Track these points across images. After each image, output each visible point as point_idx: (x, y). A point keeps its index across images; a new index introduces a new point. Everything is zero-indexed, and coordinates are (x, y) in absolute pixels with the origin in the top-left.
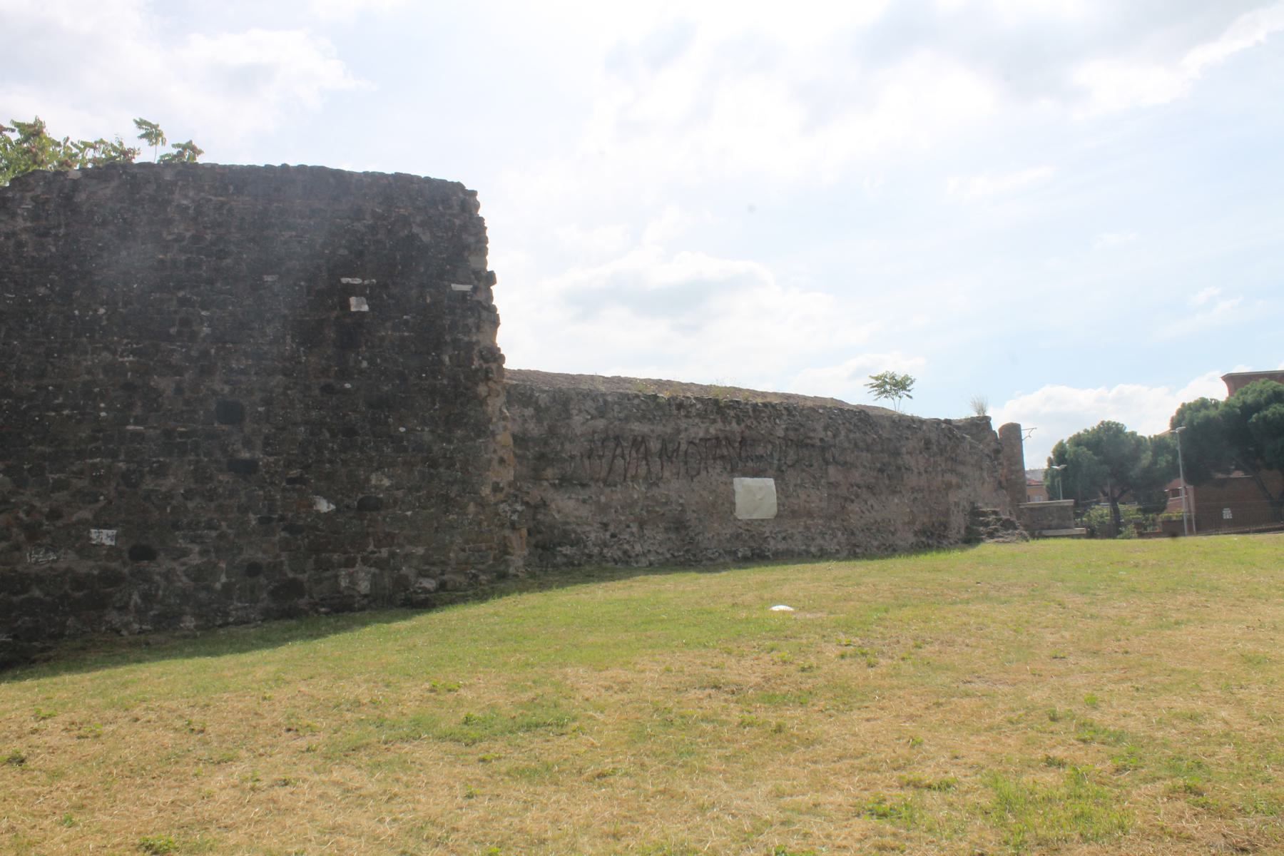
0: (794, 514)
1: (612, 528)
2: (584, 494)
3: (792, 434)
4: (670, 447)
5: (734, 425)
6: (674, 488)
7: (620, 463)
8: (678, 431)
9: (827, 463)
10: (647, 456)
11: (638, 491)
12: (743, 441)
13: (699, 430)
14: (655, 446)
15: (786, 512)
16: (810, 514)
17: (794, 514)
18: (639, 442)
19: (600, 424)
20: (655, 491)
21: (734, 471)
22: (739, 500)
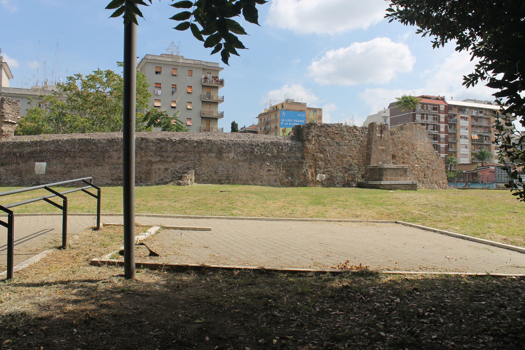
0: (50, 173)
1: (8, 176)
2: (5, 167)
3: (55, 149)
4: (22, 155)
5: (39, 148)
6: (23, 166)
7: (10, 159)
8: (24, 151)
9: (66, 157)
10: (17, 157)
11: (13, 167)
12: (40, 151)
13: (28, 150)
14: (18, 155)
15: (48, 172)
16: (55, 173)
17: (50, 173)
18: (15, 154)
19: (8, 150)
20: (18, 167)
21: (36, 161)
22: (36, 169)
